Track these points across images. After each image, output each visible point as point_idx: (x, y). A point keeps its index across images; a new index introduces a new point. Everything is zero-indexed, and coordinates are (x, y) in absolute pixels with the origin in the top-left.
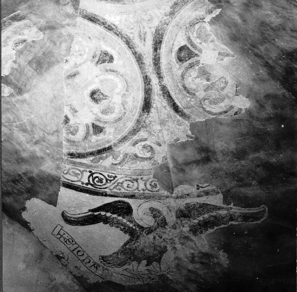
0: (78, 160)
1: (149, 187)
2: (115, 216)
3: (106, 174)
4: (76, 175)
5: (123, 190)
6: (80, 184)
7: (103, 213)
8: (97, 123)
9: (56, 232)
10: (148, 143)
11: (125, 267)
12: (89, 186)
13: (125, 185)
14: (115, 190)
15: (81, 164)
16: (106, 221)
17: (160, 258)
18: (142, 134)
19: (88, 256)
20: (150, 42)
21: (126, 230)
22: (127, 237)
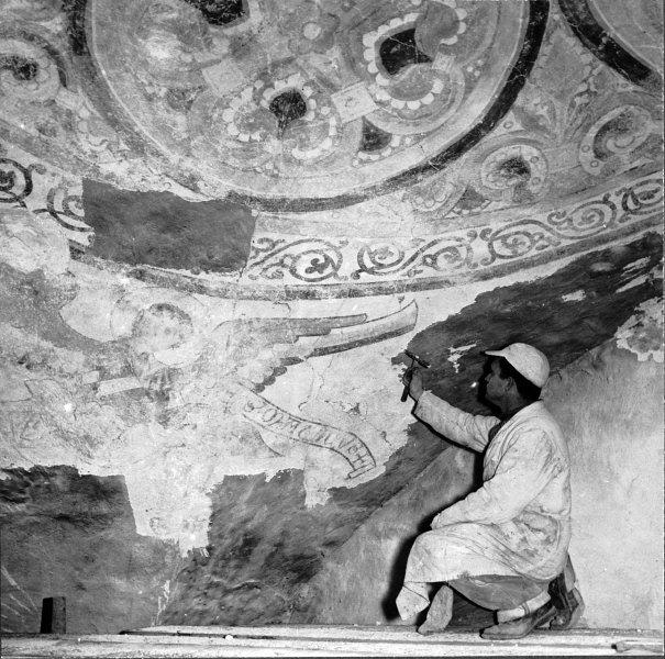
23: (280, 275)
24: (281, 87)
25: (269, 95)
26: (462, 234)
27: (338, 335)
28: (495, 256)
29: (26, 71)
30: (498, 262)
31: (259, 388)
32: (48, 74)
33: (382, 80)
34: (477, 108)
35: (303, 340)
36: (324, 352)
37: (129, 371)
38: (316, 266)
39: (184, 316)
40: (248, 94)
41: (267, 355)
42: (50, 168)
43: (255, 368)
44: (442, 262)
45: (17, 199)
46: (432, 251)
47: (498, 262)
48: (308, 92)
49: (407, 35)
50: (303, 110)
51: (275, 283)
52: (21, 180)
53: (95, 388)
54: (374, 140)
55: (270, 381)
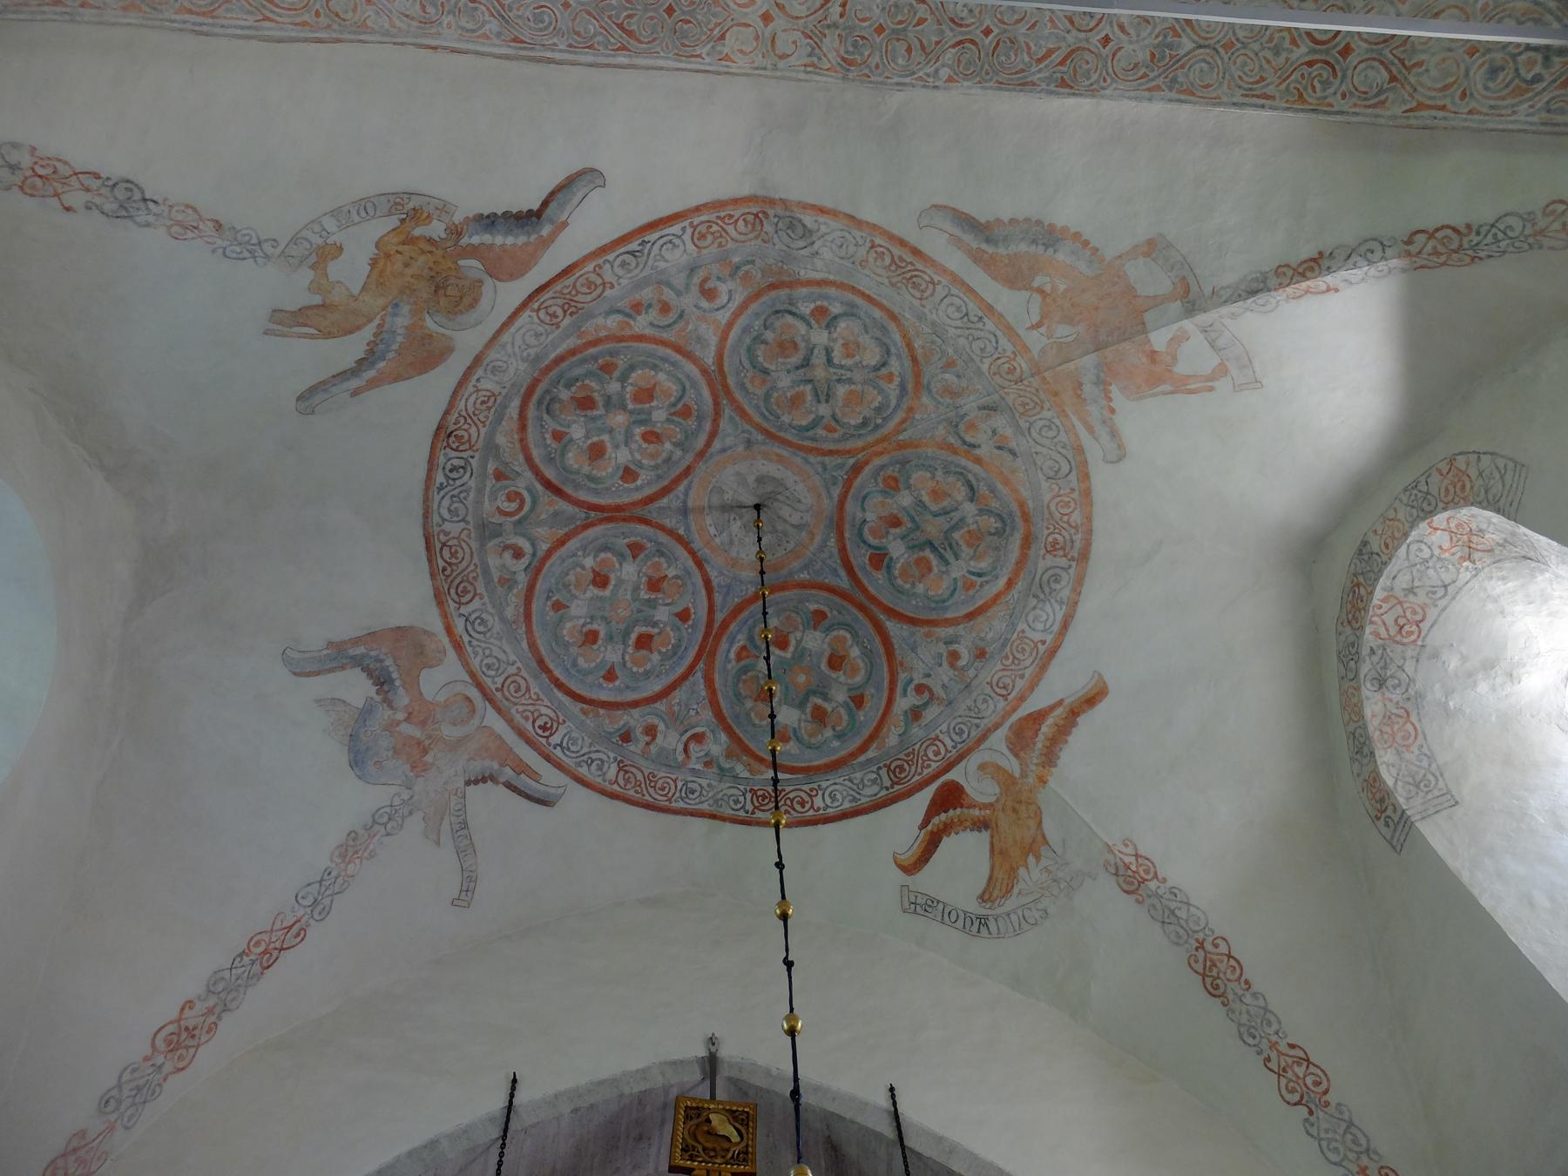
0: (862, 758)
1: (957, 738)
2: (951, 812)
3: (902, 756)
4: (874, 782)
5: (934, 765)
6: (884, 792)
7: (936, 820)
8: (854, 693)
9: (906, 905)
10: (916, 682)
11: (1016, 890)
12: (897, 787)
13: (931, 755)
14: (926, 772)
15: (869, 761)
16: (946, 829)
17: (1044, 837)
18: (902, 676)
19: (965, 913)
20: (842, 573)
21: (982, 825)
22: (985, 836)
23: (527, 718)
24: (595, 627)
25: (589, 627)
26: (612, 755)
27: (524, 781)
28: (616, 782)
29: (518, 554)
30: (615, 787)
31: (468, 783)
32: (525, 561)
33: (630, 650)
34: (657, 687)
35: (508, 770)
36: (509, 786)
37: (423, 723)
38: (544, 728)
39: (473, 711)
40: (582, 621)
41: (487, 763)
42: (486, 599)
43: (477, 767)
44: (594, 767)
45: (460, 604)
46: (594, 756)
47: (615, 787)
48: (602, 634)
49: (650, 637)
50: (594, 642)
51: (523, 721)
52: (468, 597)
53: (399, 723)
54: (610, 676)
55: (476, 782)
